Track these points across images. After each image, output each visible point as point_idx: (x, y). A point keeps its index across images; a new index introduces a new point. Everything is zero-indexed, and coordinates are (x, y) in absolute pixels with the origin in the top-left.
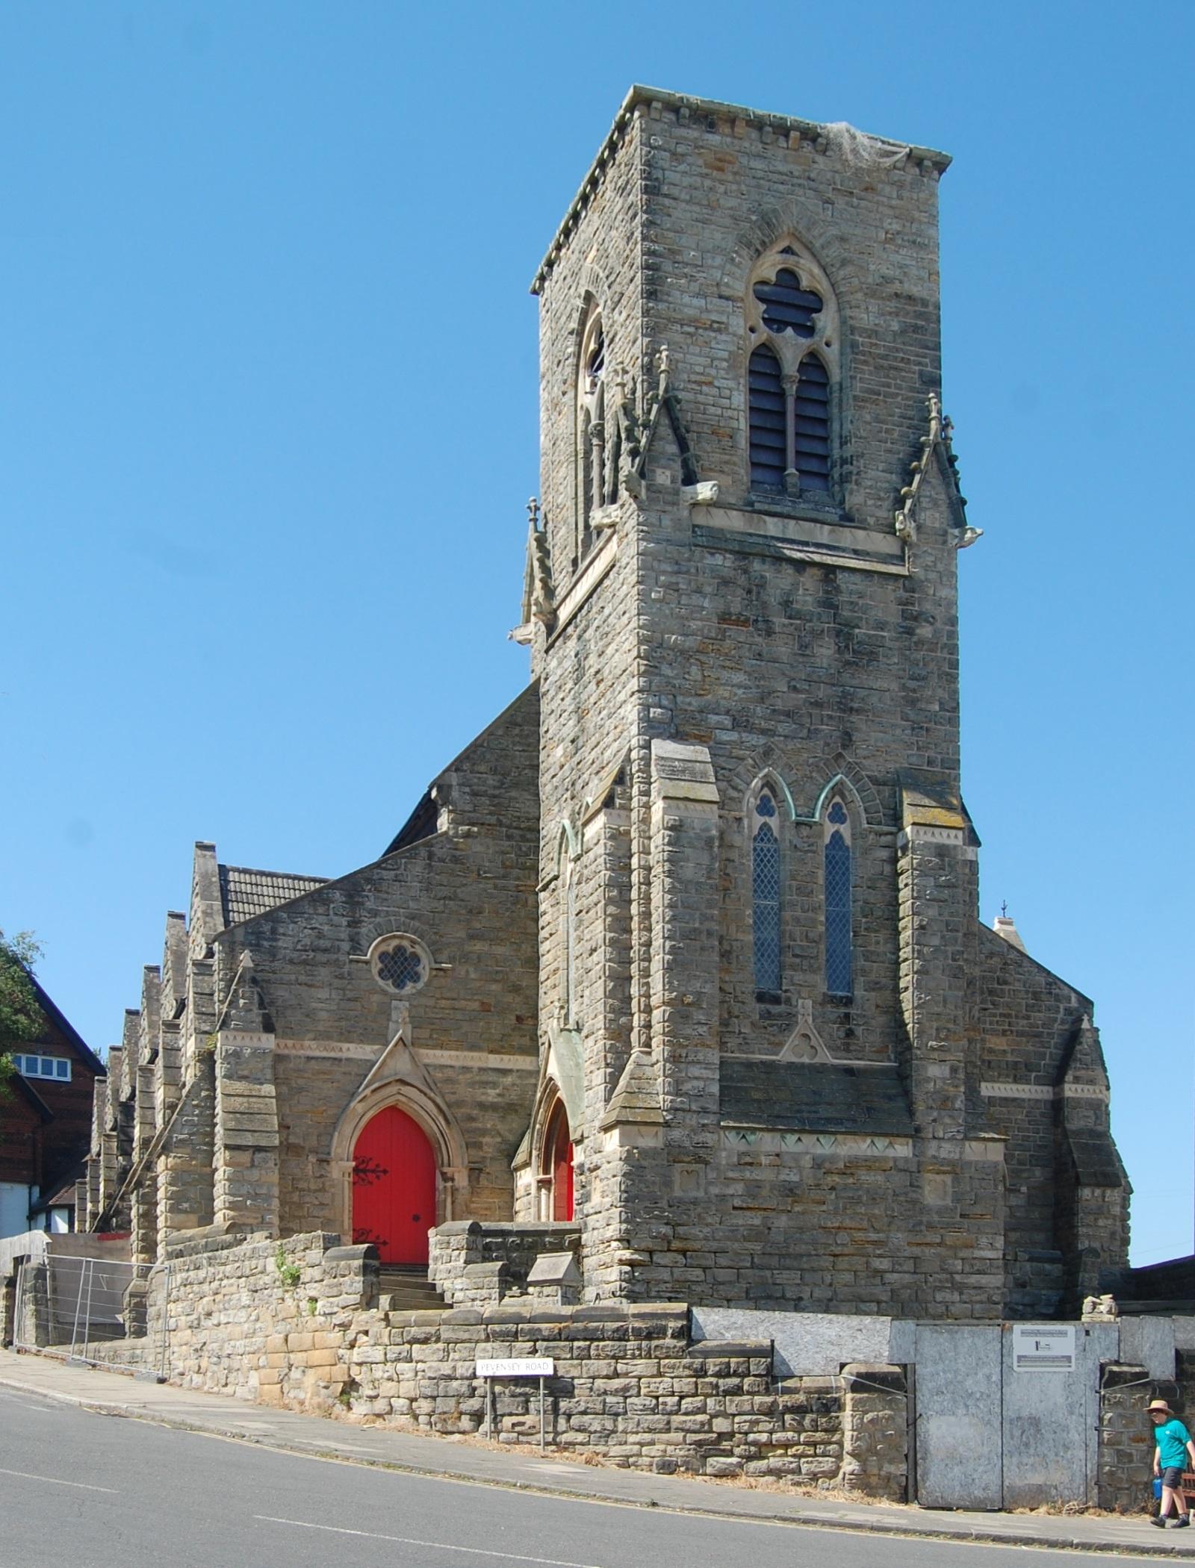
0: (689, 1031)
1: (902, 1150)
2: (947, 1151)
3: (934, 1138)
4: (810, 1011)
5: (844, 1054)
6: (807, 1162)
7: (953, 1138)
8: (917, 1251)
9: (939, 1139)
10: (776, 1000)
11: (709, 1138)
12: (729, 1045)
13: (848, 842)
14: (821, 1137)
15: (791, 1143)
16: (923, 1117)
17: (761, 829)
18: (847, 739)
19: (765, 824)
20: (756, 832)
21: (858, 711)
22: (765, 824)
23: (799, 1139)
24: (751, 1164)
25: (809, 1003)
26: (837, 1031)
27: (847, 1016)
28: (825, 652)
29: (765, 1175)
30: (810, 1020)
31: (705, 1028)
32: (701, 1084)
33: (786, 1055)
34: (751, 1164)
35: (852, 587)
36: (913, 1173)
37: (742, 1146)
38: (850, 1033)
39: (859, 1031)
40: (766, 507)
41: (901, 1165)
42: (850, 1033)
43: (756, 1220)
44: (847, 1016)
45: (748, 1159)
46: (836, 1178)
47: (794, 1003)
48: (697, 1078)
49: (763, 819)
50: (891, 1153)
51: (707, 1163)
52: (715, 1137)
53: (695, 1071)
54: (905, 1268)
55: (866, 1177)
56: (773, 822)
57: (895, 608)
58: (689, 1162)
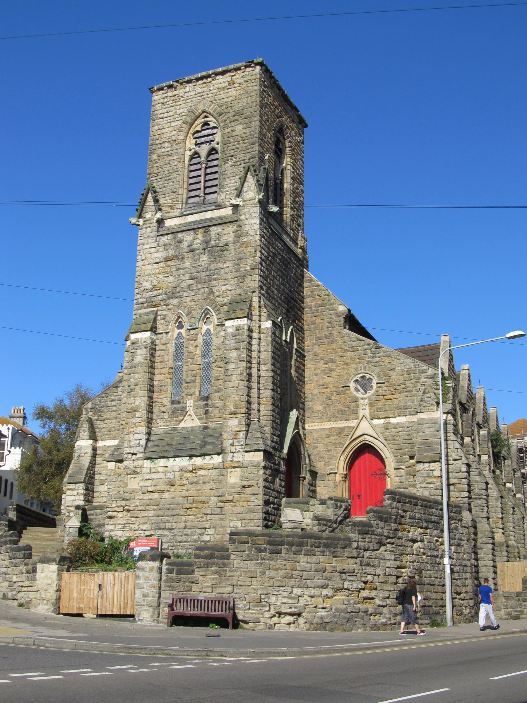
0: (134, 421)
1: (217, 459)
2: (238, 457)
3: (231, 452)
4: (192, 405)
5: (205, 421)
6: (177, 469)
7: (239, 452)
8: (221, 504)
9: (233, 453)
10: (179, 402)
11: (139, 463)
12: (159, 424)
13: (212, 332)
14: (183, 458)
15: (171, 462)
16: (227, 444)
17: (178, 334)
18: (211, 292)
19: (180, 332)
20: (175, 336)
21: (215, 280)
22: (180, 332)
23: (175, 460)
24: (155, 472)
25: (192, 401)
26: (202, 411)
27: (207, 405)
28: (204, 259)
29: (161, 475)
30: (191, 409)
31: (140, 419)
32: (137, 442)
33: (182, 425)
34: (155, 472)
35: (216, 232)
36: (221, 468)
37: (152, 465)
38: (207, 412)
39: (210, 410)
40: (188, 212)
41: (216, 466)
42: (207, 412)
43: (156, 495)
44: (207, 405)
45: (154, 471)
46: (189, 475)
47: (185, 402)
48: (136, 440)
49: (179, 331)
50: (212, 461)
51: (138, 473)
52: (142, 463)
53: (136, 436)
54: (216, 513)
55: (200, 473)
56: (183, 331)
57: (232, 235)
58: (132, 474)
